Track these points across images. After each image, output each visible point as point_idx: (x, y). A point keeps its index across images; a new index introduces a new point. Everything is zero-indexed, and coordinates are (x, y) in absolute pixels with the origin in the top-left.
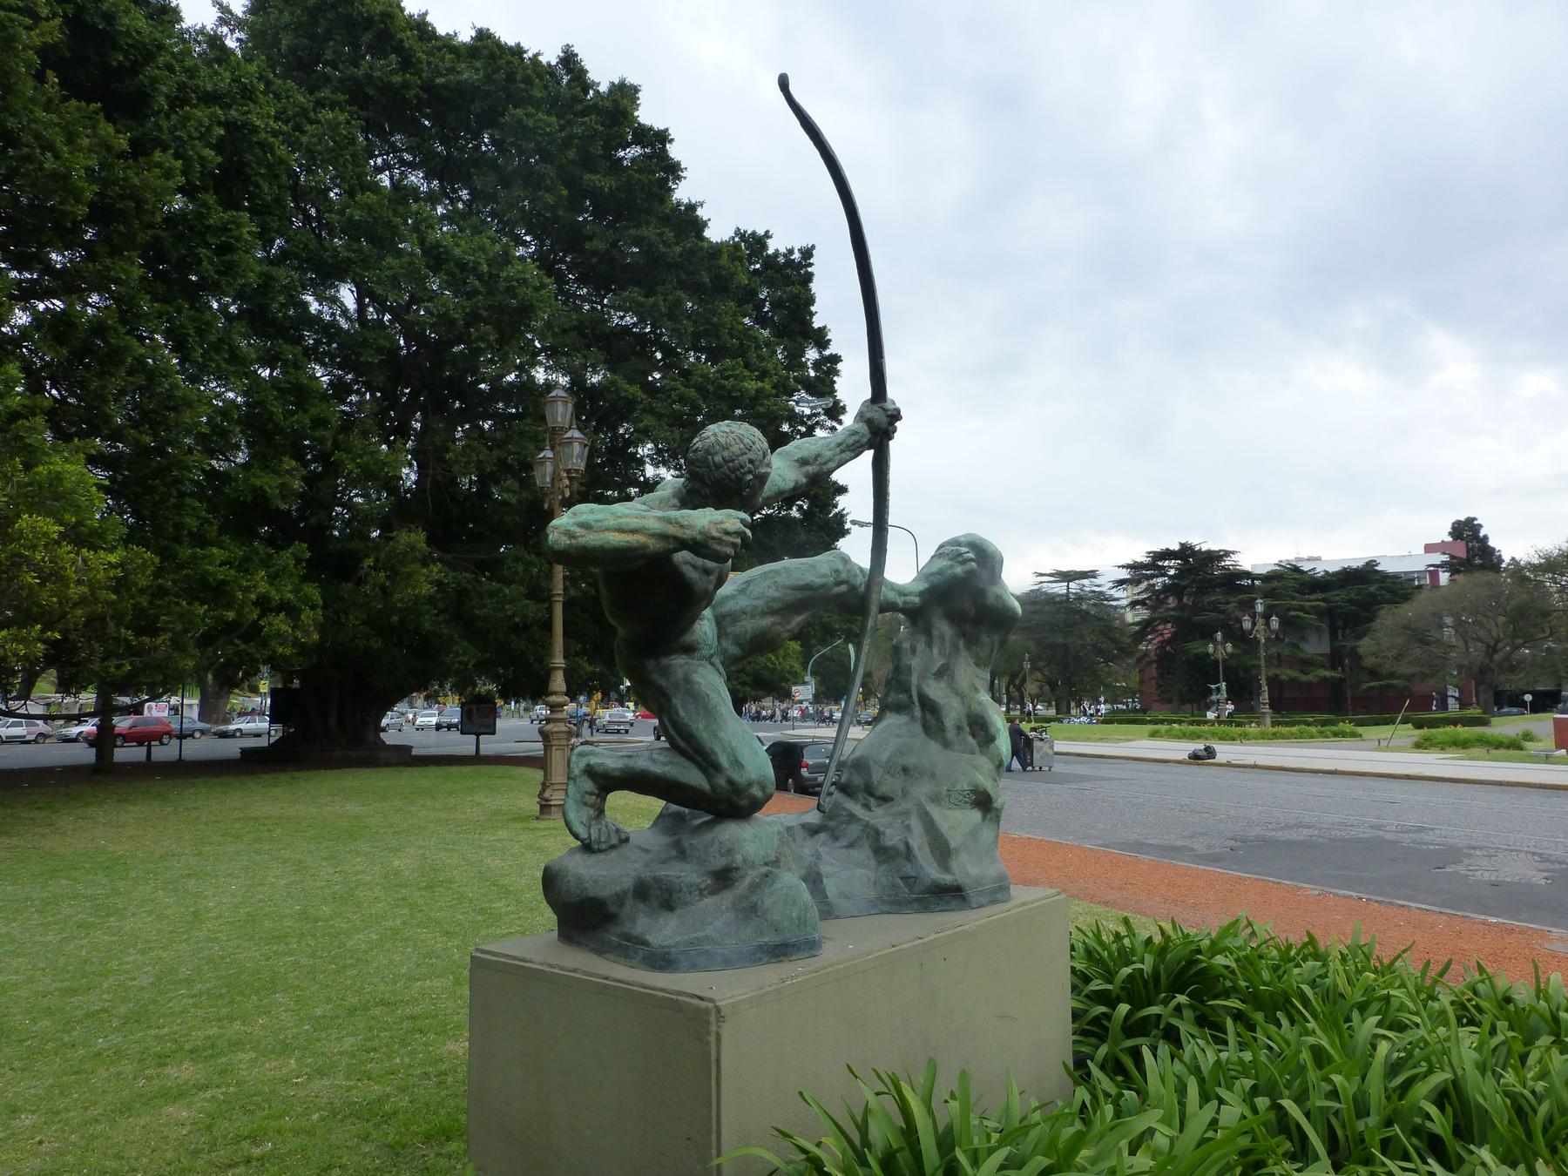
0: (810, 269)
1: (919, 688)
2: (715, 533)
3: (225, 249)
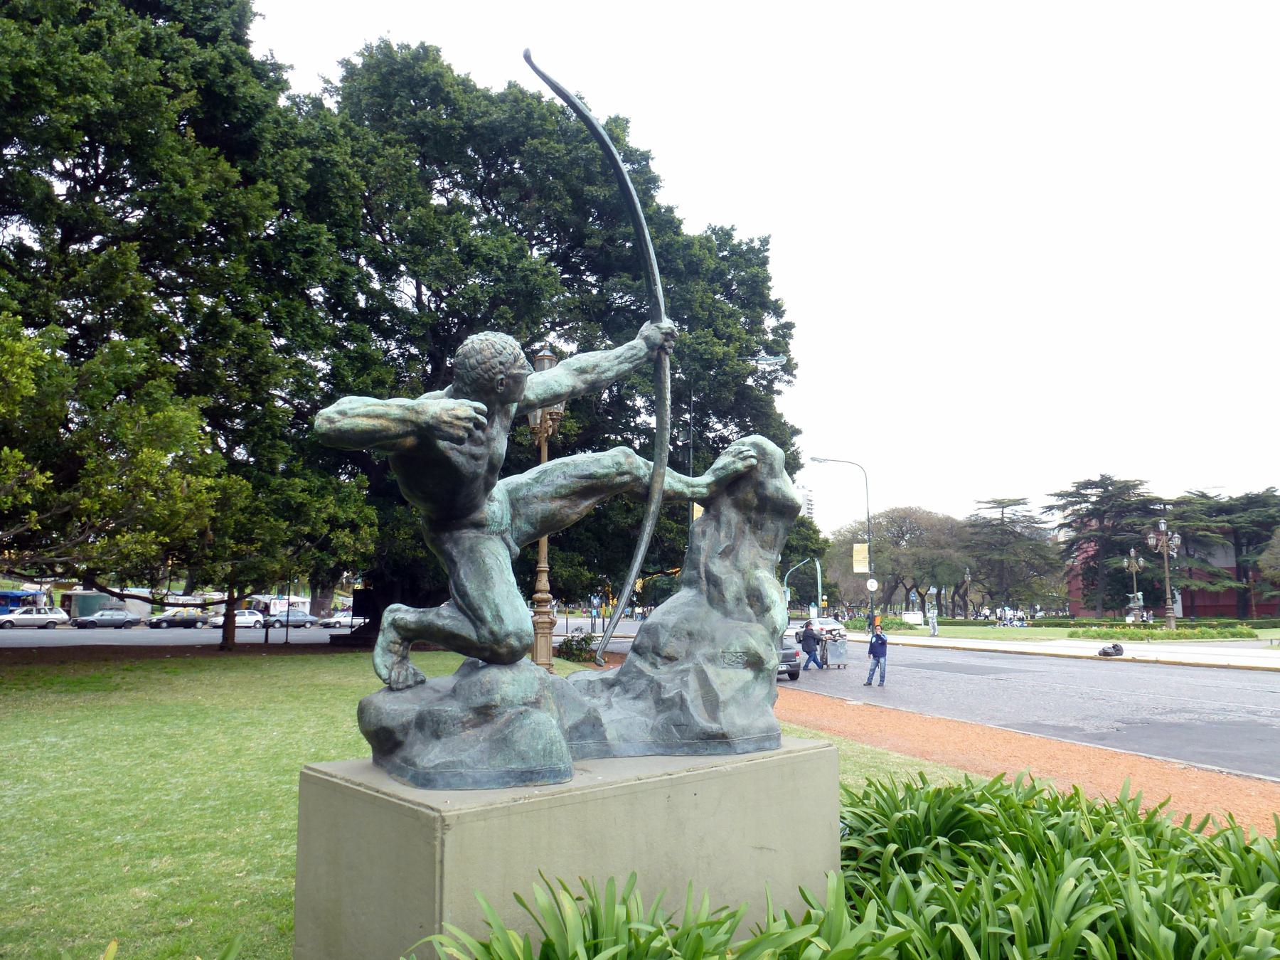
0: (766, 254)
1: (706, 566)
2: (446, 418)
3: (308, 253)
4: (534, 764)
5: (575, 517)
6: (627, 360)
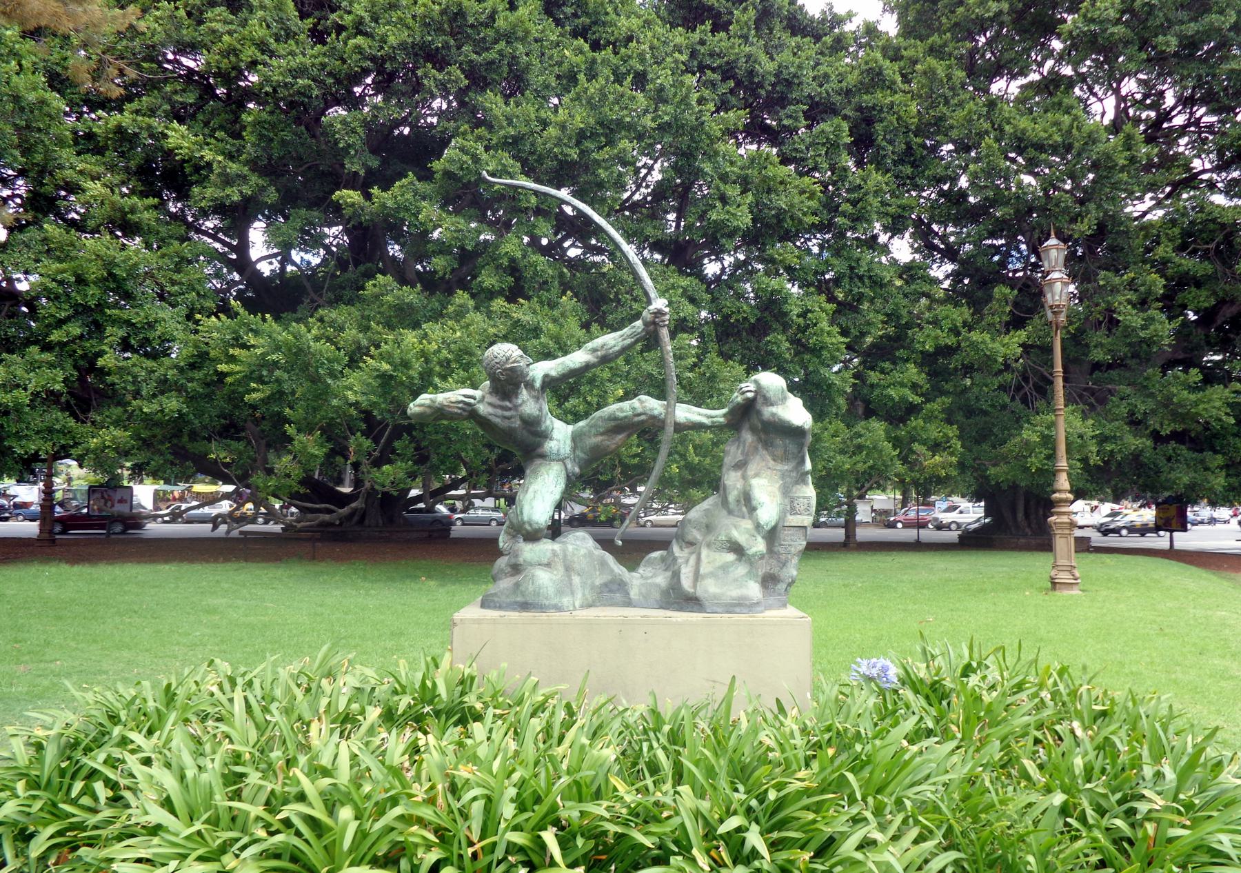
4: (530, 599)
5: (613, 447)
6: (629, 337)
